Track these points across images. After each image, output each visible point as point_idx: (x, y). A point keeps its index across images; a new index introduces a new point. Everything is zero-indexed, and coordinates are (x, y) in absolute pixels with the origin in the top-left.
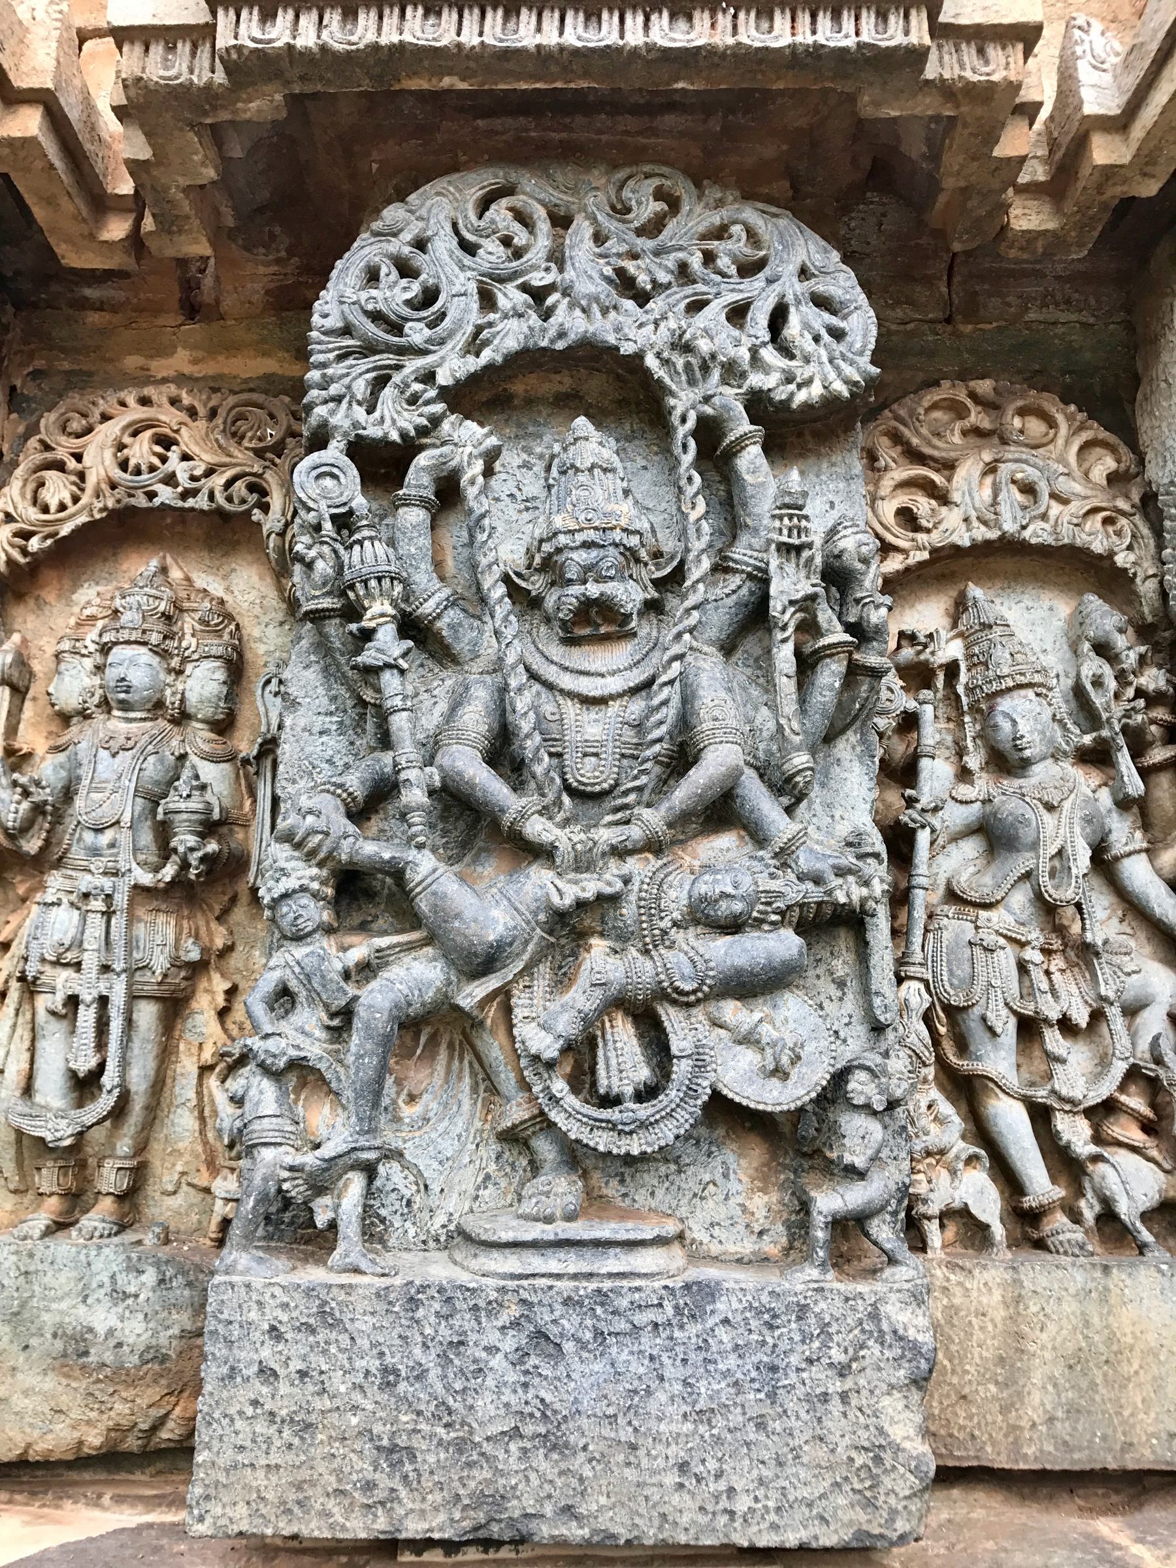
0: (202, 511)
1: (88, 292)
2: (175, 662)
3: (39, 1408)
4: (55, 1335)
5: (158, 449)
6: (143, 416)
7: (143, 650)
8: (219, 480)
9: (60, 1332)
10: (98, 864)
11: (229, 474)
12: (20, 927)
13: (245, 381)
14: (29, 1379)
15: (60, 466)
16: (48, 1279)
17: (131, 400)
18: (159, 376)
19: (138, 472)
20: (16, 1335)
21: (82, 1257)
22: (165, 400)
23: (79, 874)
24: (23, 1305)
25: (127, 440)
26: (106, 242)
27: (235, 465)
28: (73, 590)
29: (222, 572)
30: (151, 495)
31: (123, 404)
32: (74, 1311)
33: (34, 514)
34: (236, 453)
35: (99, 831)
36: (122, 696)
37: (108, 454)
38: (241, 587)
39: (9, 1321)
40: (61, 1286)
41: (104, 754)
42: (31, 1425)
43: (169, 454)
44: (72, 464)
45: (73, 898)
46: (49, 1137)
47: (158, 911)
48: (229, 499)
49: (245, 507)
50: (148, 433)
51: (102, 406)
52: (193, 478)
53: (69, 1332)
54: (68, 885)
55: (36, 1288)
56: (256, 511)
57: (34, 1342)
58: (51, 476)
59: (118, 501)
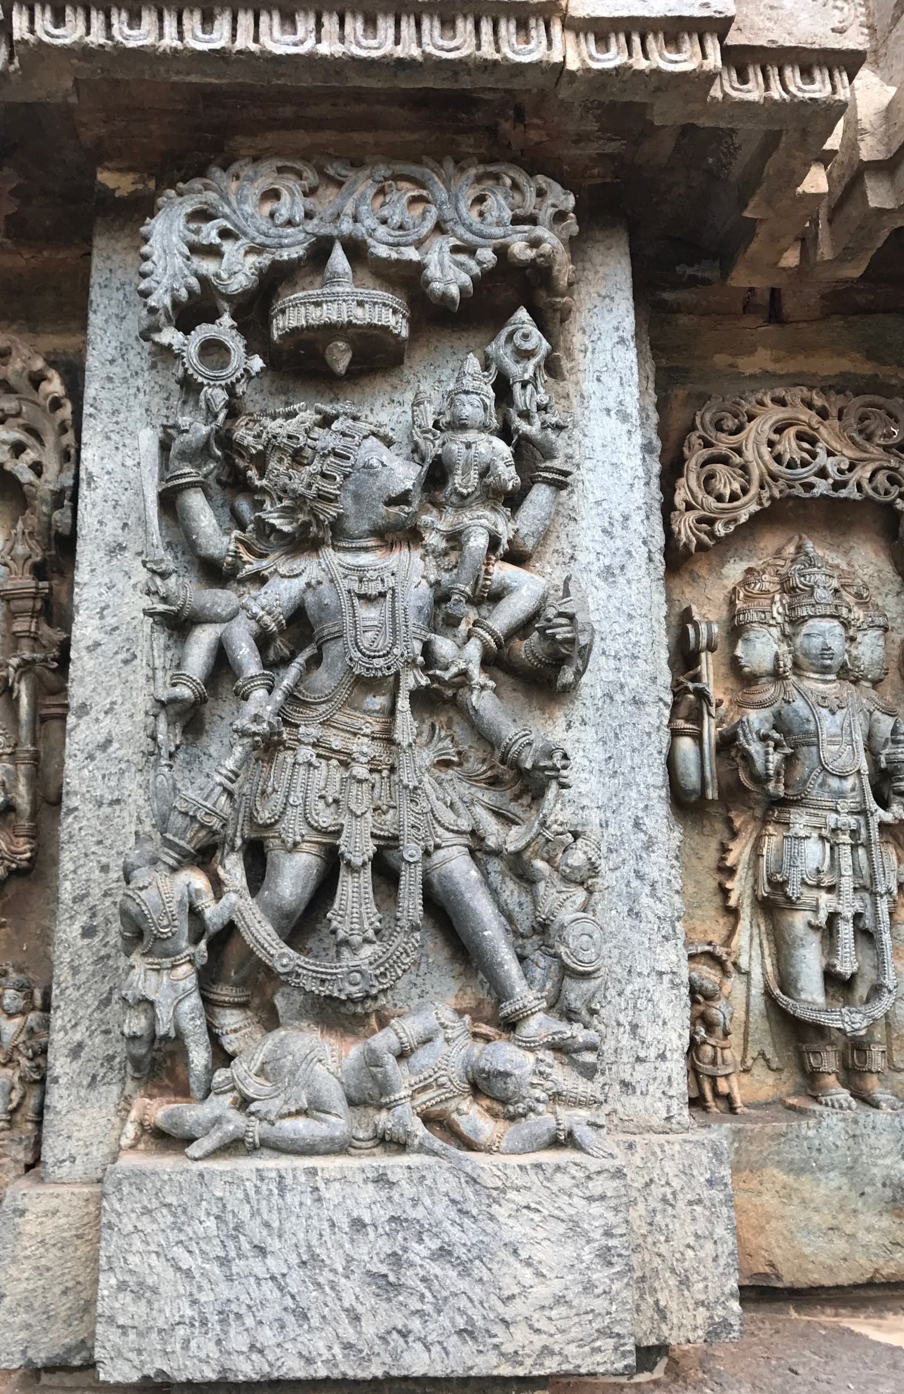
0: (855, 501)
1: (668, 296)
2: (851, 632)
3: (880, 1242)
4: (884, 1185)
5: (806, 445)
6: (786, 415)
7: (836, 623)
8: (864, 473)
9: (888, 1182)
10: (843, 805)
11: (870, 468)
12: (741, 854)
13: (825, 378)
14: (869, 1218)
15: (724, 460)
16: (872, 1140)
17: (767, 400)
18: (748, 373)
19: (791, 465)
20: (853, 1185)
21: (897, 1123)
22: (798, 401)
23: (825, 813)
24: (855, 1161)
25: (775, 437)
26: (783, 268)
27: (874, 460)
28: (723, 564)
29: (842, 549)
30: (809, 487)
31: (761, 403)
32: (897, 1166)
33: (711, 501)
34: (872, 449)
35: (843, 777)
36: (828, 662)
37: (765, 450)
38: (861, 562)
39: (845, 1174)
40: (883, 1145)
41: (825, 712)
42: (876, 1255)
43: (818, 450)
44: (737, 459)
45: (825, 833)
46: (848, 1029)
47: (887, 842)
48: (875, 489)
49: (889, 498)
50: (792, 432)
51: (746, 406)
52: (841, 471)
53: (896, 1181)
54: (815, 821)
55: (863, 1147)
56: (898, 500)
57: (868, 1190)
58: (719, 467)
59: (781, 492)
